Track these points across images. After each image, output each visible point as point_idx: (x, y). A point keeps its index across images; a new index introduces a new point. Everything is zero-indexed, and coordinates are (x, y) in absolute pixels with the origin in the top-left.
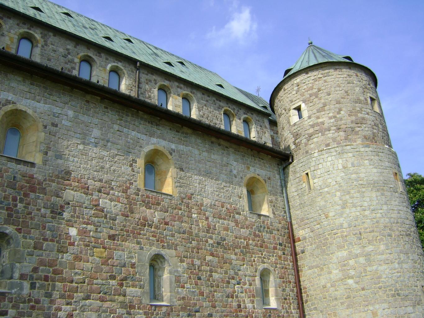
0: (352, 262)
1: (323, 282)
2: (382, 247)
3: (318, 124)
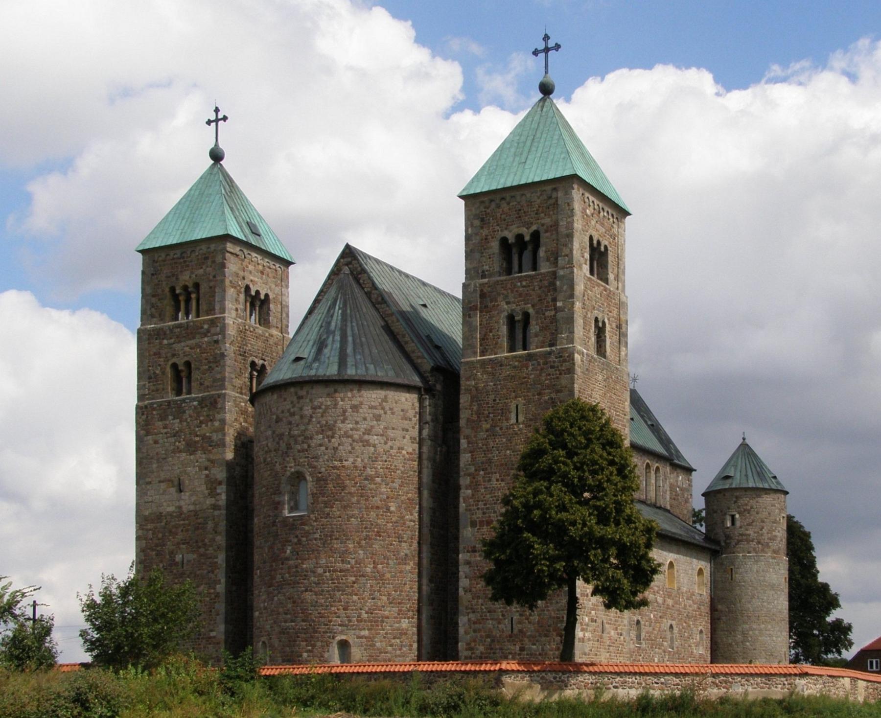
0: (751, 633)
1: (730, 641)
2: (769, 626)
3: (745, 535)
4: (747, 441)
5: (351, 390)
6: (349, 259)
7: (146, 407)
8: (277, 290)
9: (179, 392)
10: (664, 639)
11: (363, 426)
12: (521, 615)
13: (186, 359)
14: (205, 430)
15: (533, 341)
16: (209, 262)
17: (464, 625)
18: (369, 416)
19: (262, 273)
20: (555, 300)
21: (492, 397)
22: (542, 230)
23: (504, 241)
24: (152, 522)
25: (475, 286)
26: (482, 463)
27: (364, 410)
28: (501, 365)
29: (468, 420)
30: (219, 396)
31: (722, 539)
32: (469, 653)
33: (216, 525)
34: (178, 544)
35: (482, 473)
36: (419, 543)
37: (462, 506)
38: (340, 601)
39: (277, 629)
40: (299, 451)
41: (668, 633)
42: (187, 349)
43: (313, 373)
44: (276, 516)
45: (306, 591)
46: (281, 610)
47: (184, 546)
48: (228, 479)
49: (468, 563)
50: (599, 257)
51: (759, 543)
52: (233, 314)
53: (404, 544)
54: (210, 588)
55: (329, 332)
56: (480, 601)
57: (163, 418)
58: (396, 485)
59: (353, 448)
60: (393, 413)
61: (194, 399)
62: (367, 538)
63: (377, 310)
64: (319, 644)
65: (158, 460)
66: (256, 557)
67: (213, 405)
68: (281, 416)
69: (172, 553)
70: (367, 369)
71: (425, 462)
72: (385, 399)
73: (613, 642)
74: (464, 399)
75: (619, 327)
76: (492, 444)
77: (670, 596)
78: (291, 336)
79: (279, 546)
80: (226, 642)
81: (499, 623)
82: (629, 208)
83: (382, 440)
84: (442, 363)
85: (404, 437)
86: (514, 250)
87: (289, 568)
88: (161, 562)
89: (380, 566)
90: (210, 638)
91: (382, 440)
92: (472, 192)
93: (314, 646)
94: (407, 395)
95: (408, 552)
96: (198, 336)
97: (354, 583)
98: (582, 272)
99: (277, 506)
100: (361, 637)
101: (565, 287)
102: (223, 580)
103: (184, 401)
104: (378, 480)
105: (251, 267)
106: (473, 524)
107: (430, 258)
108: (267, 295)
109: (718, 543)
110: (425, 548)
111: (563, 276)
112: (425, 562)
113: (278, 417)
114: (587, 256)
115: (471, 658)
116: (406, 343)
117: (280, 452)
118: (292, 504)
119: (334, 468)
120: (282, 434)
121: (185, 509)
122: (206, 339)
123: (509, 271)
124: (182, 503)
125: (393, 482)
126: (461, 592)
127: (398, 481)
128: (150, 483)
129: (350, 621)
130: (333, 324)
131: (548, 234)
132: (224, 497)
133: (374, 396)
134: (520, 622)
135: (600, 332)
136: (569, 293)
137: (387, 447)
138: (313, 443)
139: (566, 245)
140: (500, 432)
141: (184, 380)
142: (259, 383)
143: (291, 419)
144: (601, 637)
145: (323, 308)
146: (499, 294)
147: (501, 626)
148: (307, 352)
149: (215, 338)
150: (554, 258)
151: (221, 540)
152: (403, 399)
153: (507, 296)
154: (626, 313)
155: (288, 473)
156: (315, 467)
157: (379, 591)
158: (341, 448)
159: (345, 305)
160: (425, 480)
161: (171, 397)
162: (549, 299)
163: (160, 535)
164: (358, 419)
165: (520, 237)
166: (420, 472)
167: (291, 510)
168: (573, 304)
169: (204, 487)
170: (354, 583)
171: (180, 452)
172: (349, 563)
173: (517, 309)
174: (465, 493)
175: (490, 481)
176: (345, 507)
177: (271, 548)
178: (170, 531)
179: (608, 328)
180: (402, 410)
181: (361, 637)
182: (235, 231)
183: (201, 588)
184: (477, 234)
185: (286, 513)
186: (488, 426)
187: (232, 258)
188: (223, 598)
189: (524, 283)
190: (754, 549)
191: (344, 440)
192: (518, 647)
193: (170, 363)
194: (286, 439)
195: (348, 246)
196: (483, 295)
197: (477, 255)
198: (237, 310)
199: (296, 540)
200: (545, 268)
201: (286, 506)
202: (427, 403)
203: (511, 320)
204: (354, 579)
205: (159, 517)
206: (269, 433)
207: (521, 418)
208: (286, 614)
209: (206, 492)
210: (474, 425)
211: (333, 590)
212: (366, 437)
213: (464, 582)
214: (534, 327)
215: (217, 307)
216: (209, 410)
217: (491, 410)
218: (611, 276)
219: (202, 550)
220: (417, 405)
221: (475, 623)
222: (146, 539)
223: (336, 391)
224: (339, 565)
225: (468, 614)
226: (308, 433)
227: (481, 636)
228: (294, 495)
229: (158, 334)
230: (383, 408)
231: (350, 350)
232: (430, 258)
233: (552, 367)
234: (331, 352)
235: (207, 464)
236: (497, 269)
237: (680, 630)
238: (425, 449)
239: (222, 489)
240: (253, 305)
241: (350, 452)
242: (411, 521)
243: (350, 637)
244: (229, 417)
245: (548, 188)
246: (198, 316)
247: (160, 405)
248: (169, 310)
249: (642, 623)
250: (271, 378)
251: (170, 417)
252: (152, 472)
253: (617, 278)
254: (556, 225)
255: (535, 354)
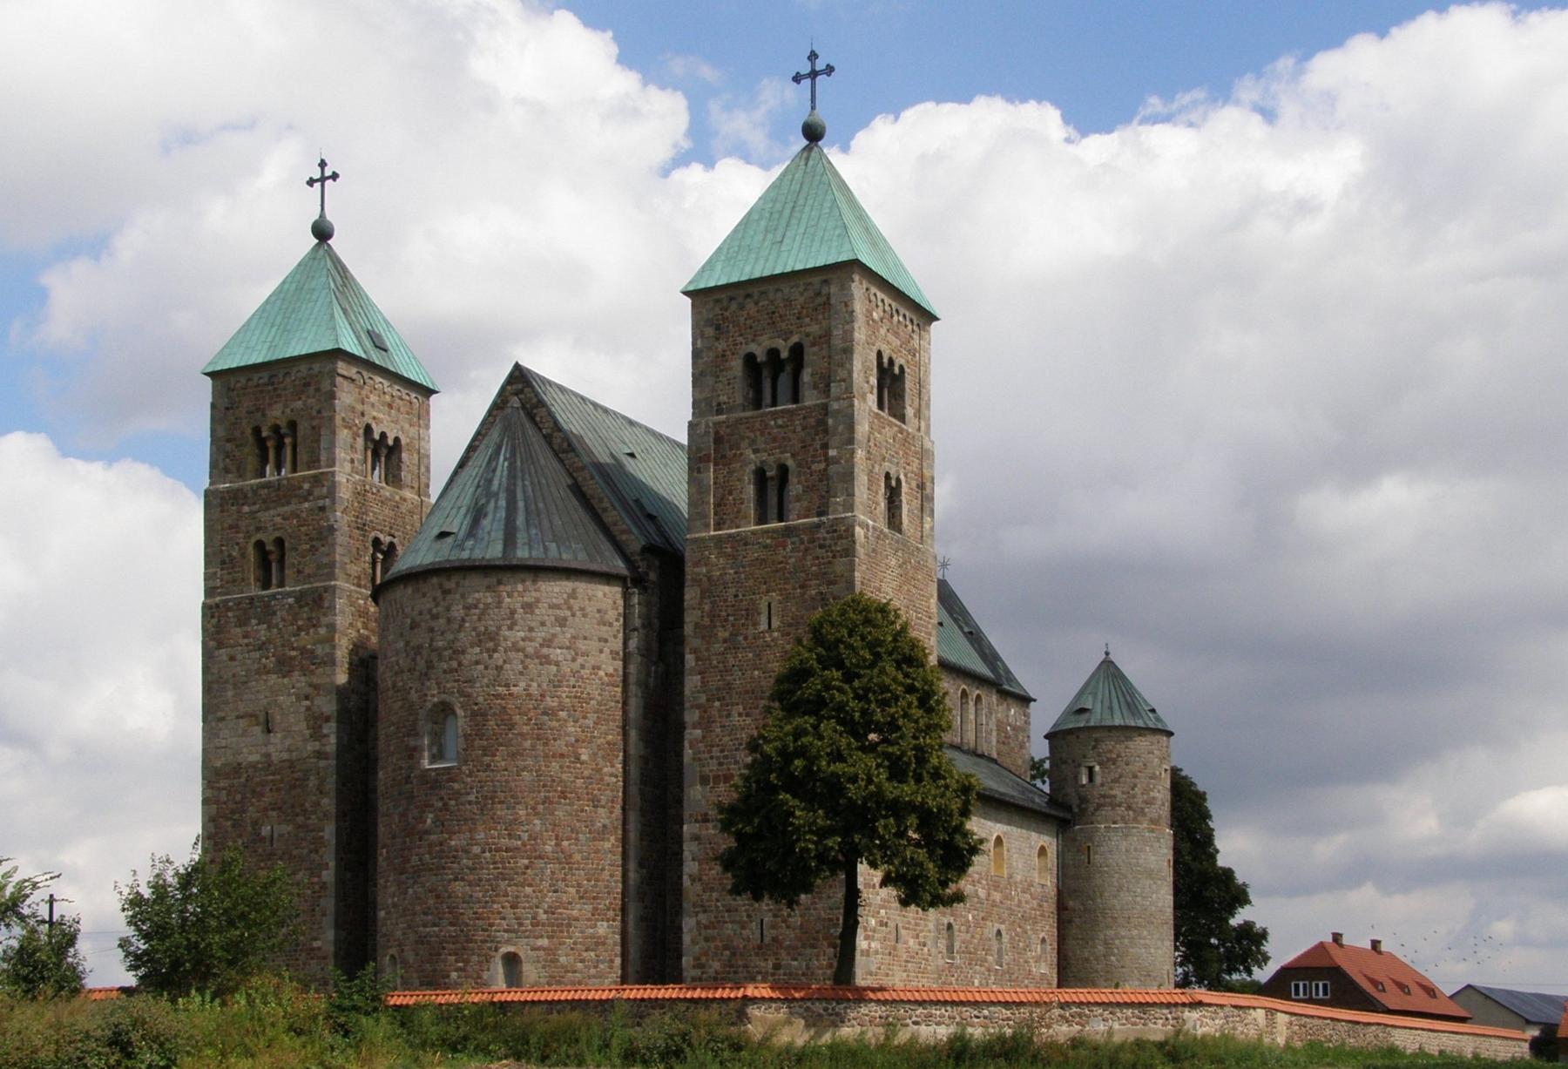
4: (1112, 657)
5: (523, 581)
6: (520, 386)
7: (217, 606)
8: (413, 431)
9: (266, 584)
10: (988, 951)
11: (540, 634)
12: (775, 916)
13: (277, 534)
14: (305, 639)
15: (794, 507)
16: (311, 390)
17: (690, 931)
18: (549, 620)
19: (390, 406)
20: (825, 446)
21: (732, 591)
22: (806, 342)
23: (750, 359)
24: (227, 776)
25: (707, 426)
26: (718, 689)
27: (542, 611)
28: (746, 544)
29: (697, 625)
30: (326, 589)
31: (1075, 802)
32: (699, 972)
33: (322, 781)
34: (266, 809)
35: (717, 704)
36: (623, 809)
37: (688, 753)
38: (506, 895)
39: (412, 937)
40: (445, 672)
41: (995, 945)
42: (278, 520)
43: (465, 555)
44: (411, 768)
45: (456, 879)
46: (418, 908)
47: (274, 813)
48: (339, 712)
49: (696, 838)
50: (892, 384)
51: (1129, 808)
52: (347, 467)
53: (600, 810)
54: (312, 875)
55: (490, 495)
56: (715, 895)
57: (242, 622)
58: (589, 722)
59: (525, 668)
60: (585, 616)
61: (289, 594)
62: (546, 800)
63: (561, 461)
64: (475, 958)
65: (235, 685)
66: (381, 829)
67: (317, 602)
68: (418, 619)
69: (255, 823)
70: (546, 549)
71: (633, 688)
72: (573, 595)
73: (912, 956)
74: (691, 595)
75: (922, 487)
76: (731, 661)
77: (997, 887)
78: (433, 500)
79: (416, 812)
80: (336, 955)
81: (743, 928)
82: (936, 311)
83: (569, 655)
84: (658, 540)
85: (601, 651)
86: (765, 373)
87: (430, 846)
88: (240, 836)
89: (565, 843)
90: (313, 949)
91: (569, 655)
92: (702, 286)
93: (467, 962)
94: (607, 588)
95: (607, 822)
96: (294, 500)
97: (527, 867)
98: (866, 405)
99: (413, 753)
100: (538, 949)
101: (841, 428)
102: (332, 864)
103: (274, 596)
104: (563, 714)
105: (373, 398)
106: (704, 780)
107: (640, 385)
108: (397, 440)
109: (1069, 808)
110: (633, 816)
111: (838, 411)
112: (633, 836)
113: (413, 621)
114: (874, 381)
115: (700, 979)
116: (605, 510)
117: (417, 674)
118: (435, 750)
119: (498, 696)
120: (420, 647)
121: (275, 758)
122: (306, 505)
123: (758, 404)
124: (271, 749)
125: (585, 717)
126: (686, 881)
127: (592, 717)
128: (222, 719)
129: (521, 925)
130: (496, 483)
131: (815, 349)
132: (333, 739)
133: (557, 589)
134: (773, 927)
135: (893, 494)
136: (846, 436)
137: (576, 666)
138: (467, 659)
139: (842, 365)
140: (744, 644)
141: (274, 565)
142: (385, 570)
143: (433, 624)
144: (895, 949)
145: (480, 459)
146: (743, 438)
147: (746, 932)
148: (457, 523)
149: (321, 503)
150: (824, 384)
151: (329, 803)
152: (600, 594)
153: (754, 442)
154: (932, 467)
155: (429, 705)
156: (468, 696)
157: (564, 880)
158: (507, 666)
159: (513, 454)
160: (632, 715)
161: (255, 591)
162: (817, 444)
163: (238, 797)
164: (533, 624)
165: (773, 353)
166: (625, 703)
167: (433, 759)
168: (853, 452)
169: (303, 725)
170: (527, 867)
171: (268, 672)
172: (519, 838)
173: (770, 460)
174: (692, 734)
175: (729, 716)
176: (513, 755)
177: (403, 815)
178: (254, 792)
179: (905, 488)
180: (599, 611)
181: (538, 949)
182: (350, 345)
183: (299, 876)
184: (710, 349)
185: (426, 764)
186: (727, 634)
187: (346, 383)
188: (331, 890)
189: (780, 422)
190: (1123, 818)
191: (512, 655)
192: (770, 964)
193: (253, 540)
194: (425, 652)
195: (517, 366)
196: (718, 440)
197: (710, 380)
198: (352, 461)
199: (440, 804)
200: (810, 399)
201: (426, 754)
202: (635, 600)
203: (760, 476)
204: (526, 862)
205: (237, 769)
206: (401, 644)
207: (776, 623)
208: (425, 914)
209: (307, 732)
210: (706, 633)
211: (496, 878)
212: (545, 651)
213: (690, 867)
214: (795, 488)
215: (323, 458)
216: (312, 610)
217: (730, 610)
218: (910, 412)
219: (300, 819)
220: (620, 602)
221: (706, 927)
222: (217, 802)
223: (499, 582)
224: (505, 842)
225: (697, 914)
226: (458, 645)
227: (716, 948)
228: (438, 738)
229: (236, 497)
230: (570, 608)
231: (520, 521)
232: (640, 385)
233: (821, 547)
234: (493, 524)
236: (739, 400)
237: (1012, 938)
238: (632, 669)
239: (330, 729)
240: (376, 454)
241: (521, 673)
242: (611, 775)
243: (521, 949)
244: (341, 621)
245: (816, 280)
246: (294, 470)
247: (238, 602)
248: (252, 462)
249: (956, 927)
250: (402, 564)
251: (254, 622)
252: (227, 703)
253: (918, 414)
254: (827, 335)
255: (796, 528)
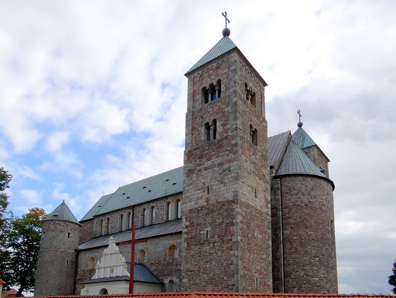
121: (258, 208)
128: (243, 182)
163: (248, 217)
183: (264, 256)
205: (248, 206)
222: (242, 216)
235: (265, 190)
